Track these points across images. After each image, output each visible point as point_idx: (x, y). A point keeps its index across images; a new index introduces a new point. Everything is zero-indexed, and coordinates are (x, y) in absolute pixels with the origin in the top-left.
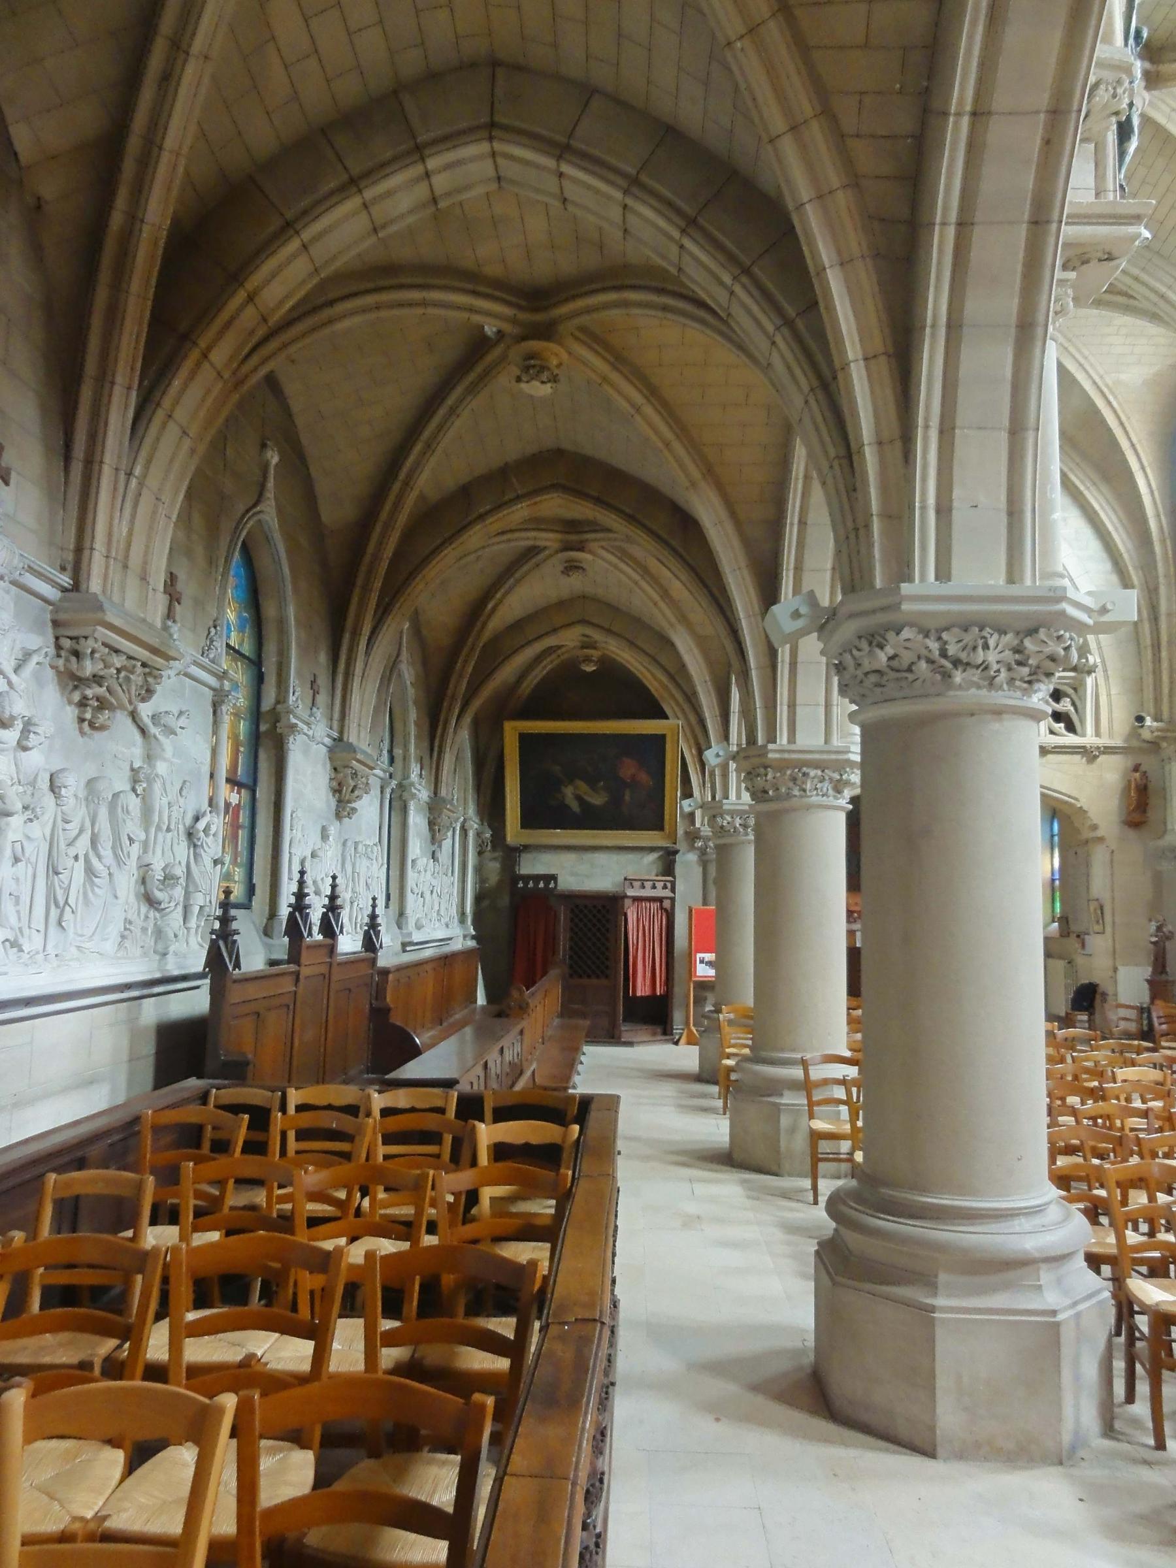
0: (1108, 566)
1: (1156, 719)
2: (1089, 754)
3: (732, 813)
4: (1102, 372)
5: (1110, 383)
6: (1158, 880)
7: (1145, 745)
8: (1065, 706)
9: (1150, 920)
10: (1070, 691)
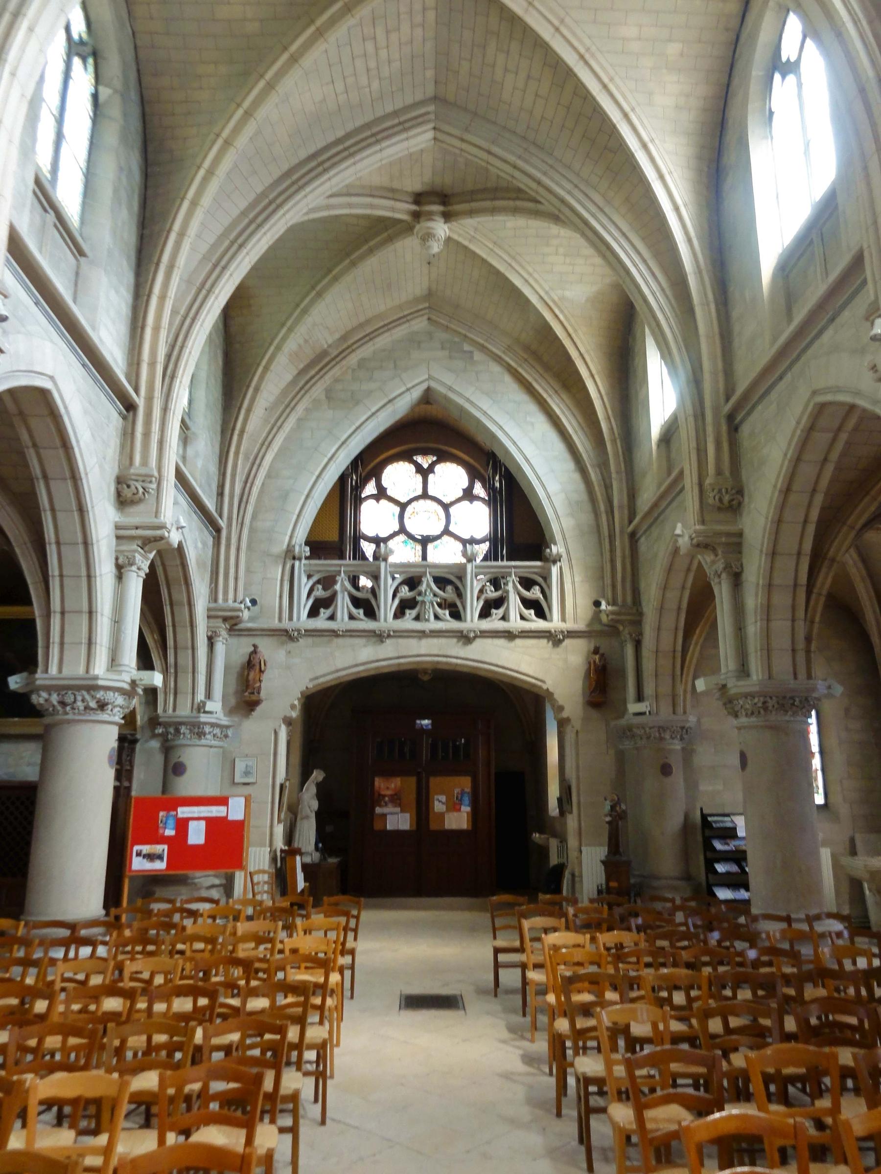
0: (571, 465)
1: (614, 603)
2: (554, 638)
3: (49, 689)
4: (547, 289)
5: (556, 298)
6: (621, 758)
7: (606, 628)
8: (535, 593)
9: (606, 799)
10: (540, 580)
